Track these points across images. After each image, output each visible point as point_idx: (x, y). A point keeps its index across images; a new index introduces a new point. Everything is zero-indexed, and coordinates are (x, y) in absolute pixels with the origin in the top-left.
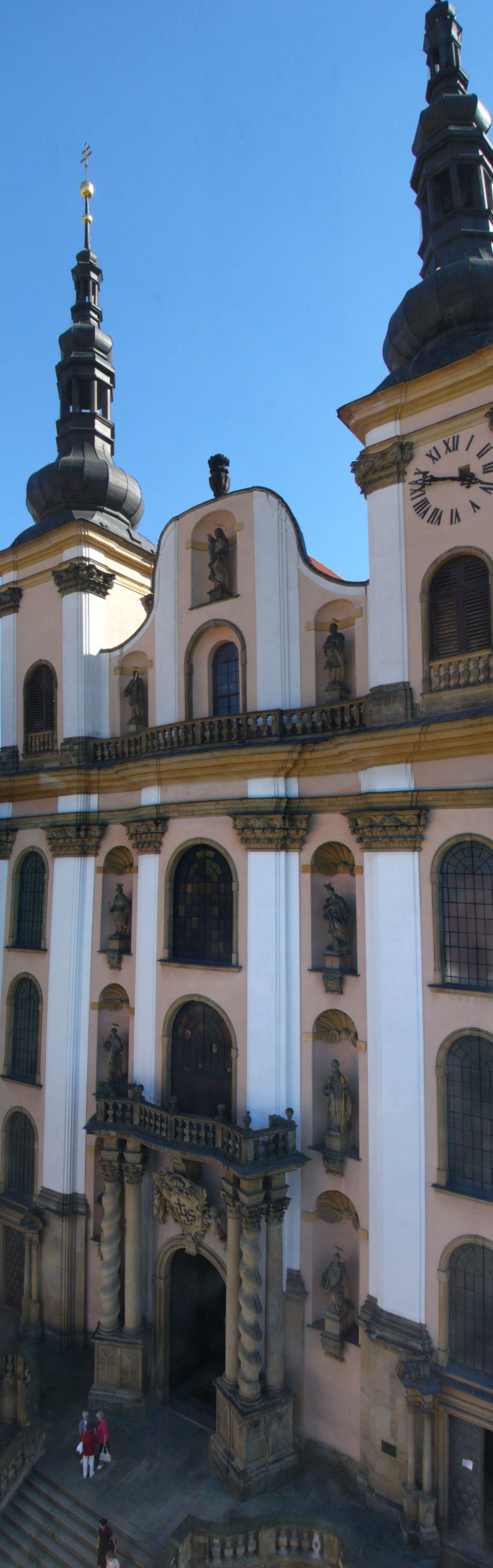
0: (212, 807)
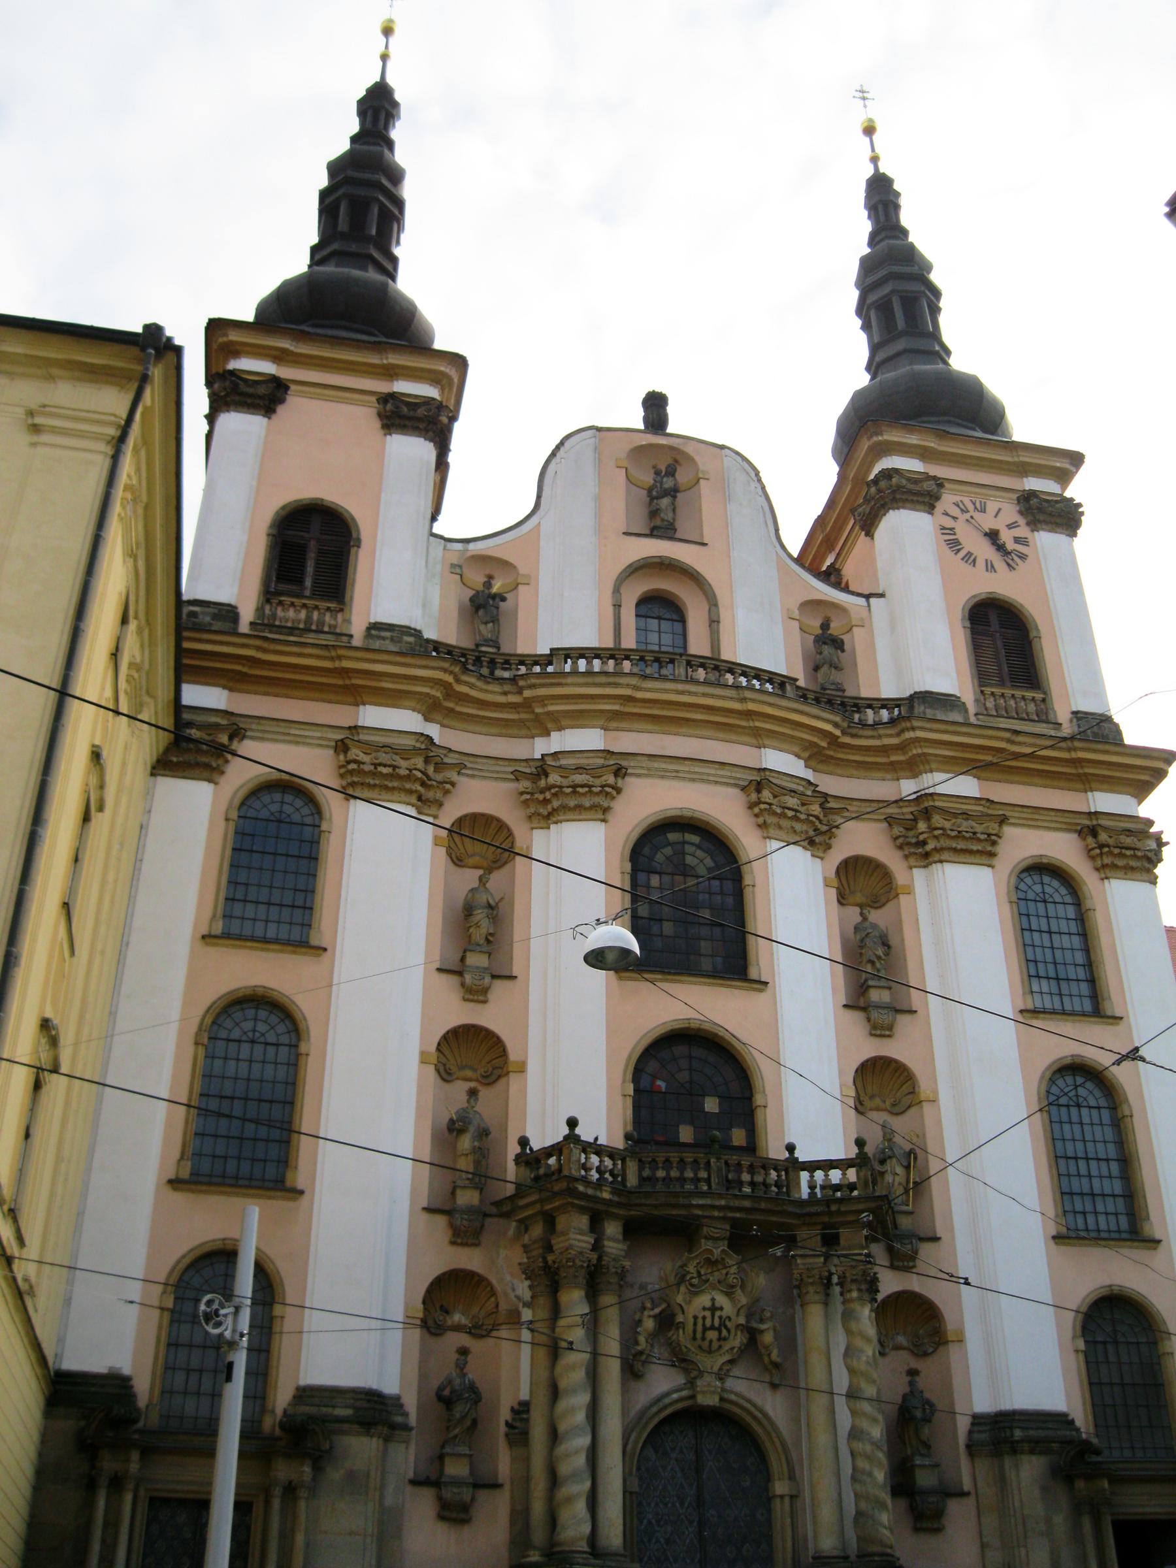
0: (713, 772)
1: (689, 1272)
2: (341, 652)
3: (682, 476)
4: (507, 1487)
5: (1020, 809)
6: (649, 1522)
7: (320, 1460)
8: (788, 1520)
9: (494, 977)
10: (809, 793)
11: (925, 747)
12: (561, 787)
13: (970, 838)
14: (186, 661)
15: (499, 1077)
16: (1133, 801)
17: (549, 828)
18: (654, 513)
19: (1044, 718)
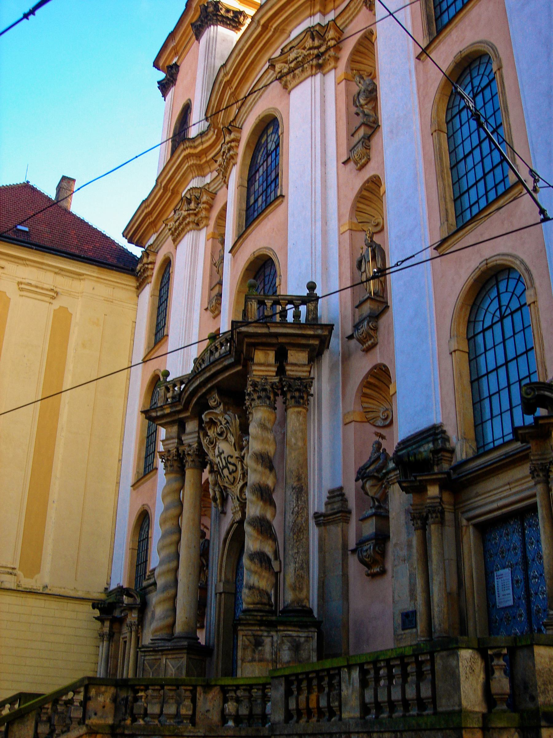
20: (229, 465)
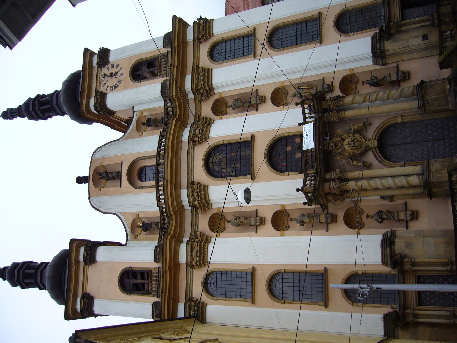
1: (339, 152)
2: (164, 270)
3: (102, 170)
4: (406, 200)
5: (194, 62)
6: (413, 158)
7: (403, 257)
8: (409, 117)
9: (257, 216)
10: (194, 126)
11: (178, 92)
12: (199, 201)
13: (204, 77)
14: (171, 318)
15: (286, 212)
16: (189, 28)
17: (211, 203)
18: (114, 178)
19: (166, 56)
20: (354, 141)
